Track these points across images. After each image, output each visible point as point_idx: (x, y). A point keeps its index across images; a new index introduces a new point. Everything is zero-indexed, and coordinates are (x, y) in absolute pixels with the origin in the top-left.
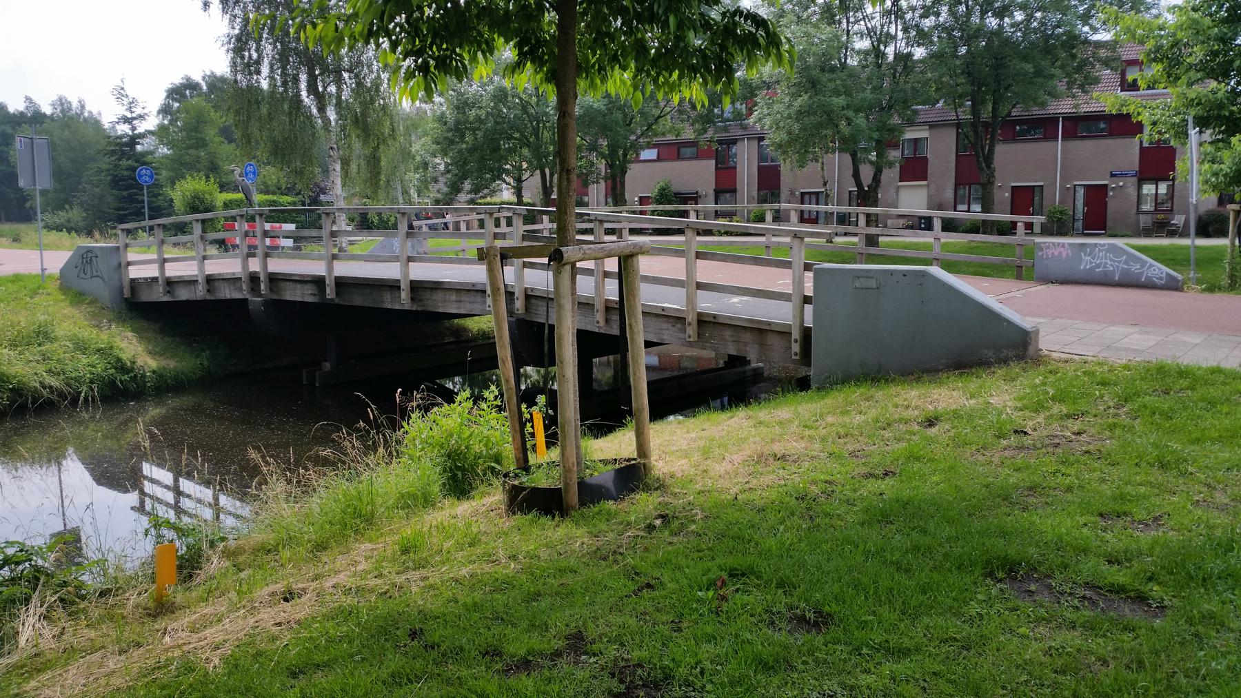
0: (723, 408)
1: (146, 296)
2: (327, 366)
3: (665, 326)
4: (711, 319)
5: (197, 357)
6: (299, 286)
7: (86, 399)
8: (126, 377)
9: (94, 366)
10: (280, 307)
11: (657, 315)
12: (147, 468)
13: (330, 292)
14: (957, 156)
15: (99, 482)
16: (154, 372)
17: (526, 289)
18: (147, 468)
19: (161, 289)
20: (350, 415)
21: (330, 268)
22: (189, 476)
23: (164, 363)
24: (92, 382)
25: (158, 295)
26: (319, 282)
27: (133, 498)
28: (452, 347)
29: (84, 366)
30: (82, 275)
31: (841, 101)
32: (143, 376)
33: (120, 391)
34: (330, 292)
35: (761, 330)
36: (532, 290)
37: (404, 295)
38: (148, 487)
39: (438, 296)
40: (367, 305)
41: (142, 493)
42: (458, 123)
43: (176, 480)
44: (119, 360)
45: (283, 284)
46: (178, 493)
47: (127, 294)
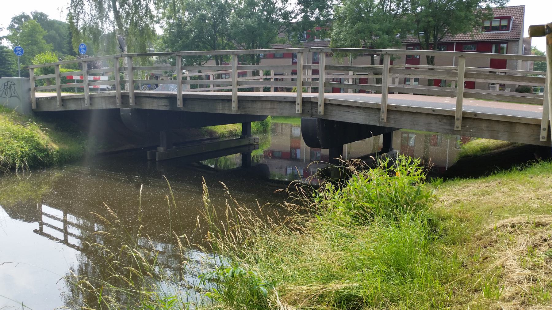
0: (521, 170)
1: (46, 108)
2: (161, 149)
3: (433, 121)
4: (473, 116)
5: (80, 144)
6: (155, 100)
7: (20, 168)
8: (42, 154)
9: (22, 148)
10: (141, 113)
11: (428, 114)
12: (45, 208)
13: (180, 104)
14: (406, 59)
15: (13, 218)
16: (58, 152)
17: (325, 99)
18: (45, 208)
19: (58, 103)
20: (506, 169)
21: (180, 91)
22: (72, 213)
23: (62, 147)
24: (22, 157)
25: (57, 107)
26: (172, 98)
27: (36, 225)
28: (208, 141)
29: (18, 147)
30: (4, 95)
31: (377, 26)
32: (52, 154)
33: (38, 162)
34: (180, 104)
35: (511, 123)
36: (330, 100)
37: (234, 105)
38: (45, 219)
39: (258, 105)
40: (204, 111)
41: (42, 224)
42: (178, 32)
43: (65, 215)
44: (38, 144)
45: (144, 99)
46: (65, 222)
47: (34, 106)
